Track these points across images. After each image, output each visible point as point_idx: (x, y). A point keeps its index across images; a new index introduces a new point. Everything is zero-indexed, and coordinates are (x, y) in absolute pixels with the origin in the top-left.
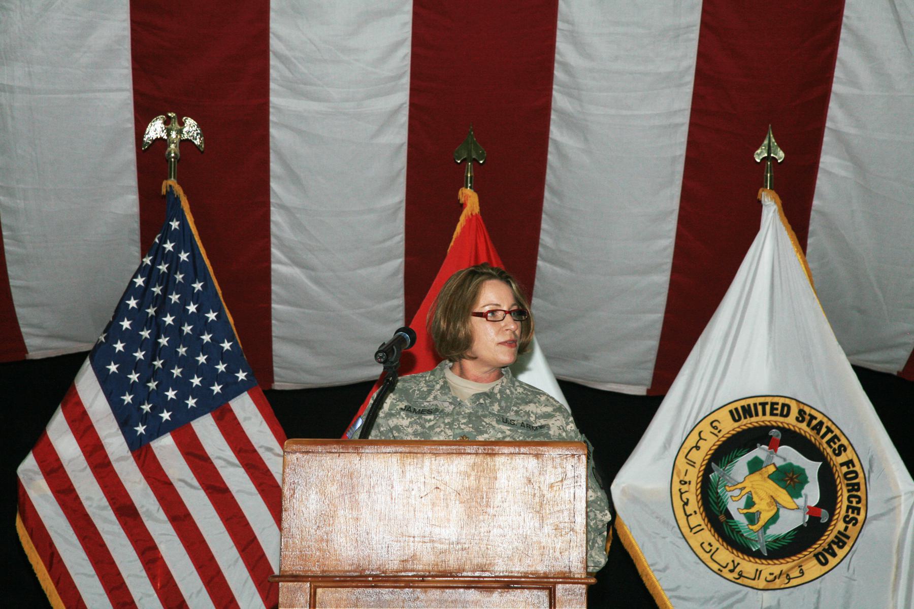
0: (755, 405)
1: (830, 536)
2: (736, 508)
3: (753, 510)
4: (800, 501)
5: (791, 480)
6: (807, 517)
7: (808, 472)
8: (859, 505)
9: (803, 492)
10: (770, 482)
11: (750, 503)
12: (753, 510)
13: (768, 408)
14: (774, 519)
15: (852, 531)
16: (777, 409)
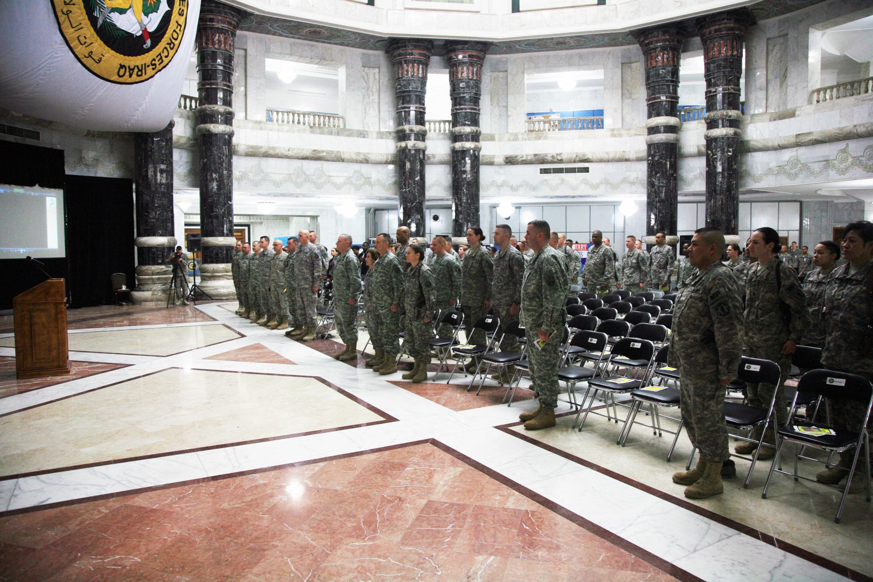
4: (145, 20)
8: (164, 59)
14: (122, 11)
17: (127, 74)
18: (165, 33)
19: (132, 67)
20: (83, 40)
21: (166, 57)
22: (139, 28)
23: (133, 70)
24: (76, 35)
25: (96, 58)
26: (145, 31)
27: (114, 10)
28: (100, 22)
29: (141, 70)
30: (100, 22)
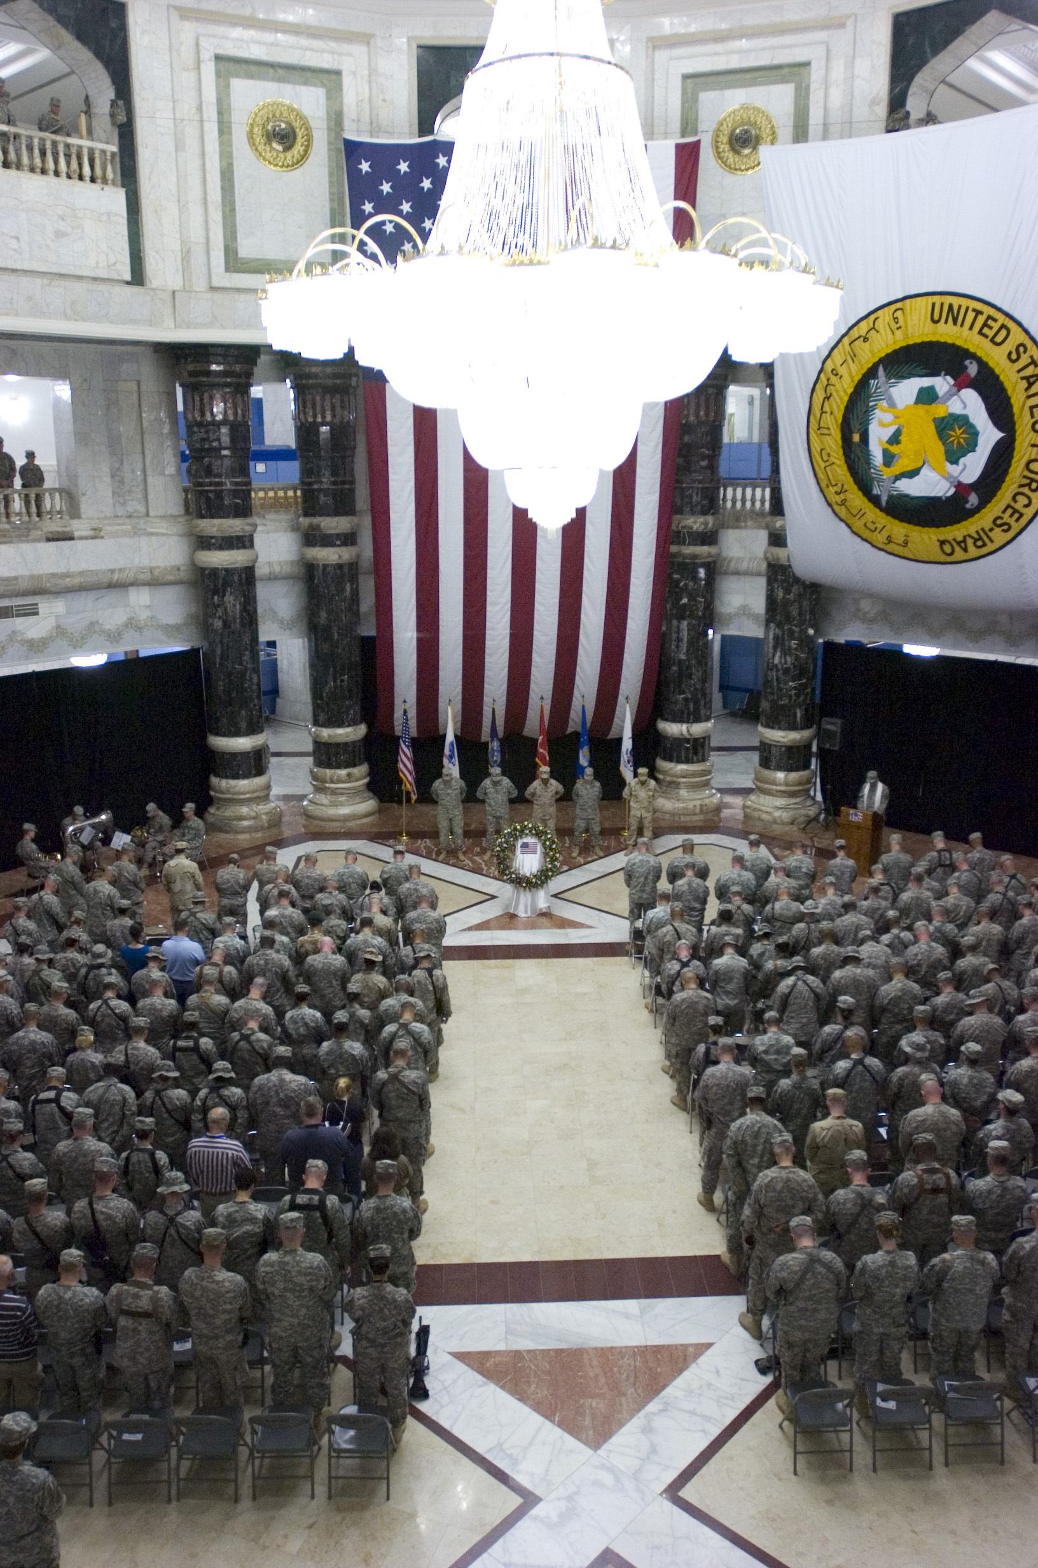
0: (967, 308)
1: (969, 527)
2: (878, 434)
3: (894, 449)
4: (954, 470)
5: (954, 436)
6: (952, 491)
7: (981, 440)
8: (1024, 510)
9: (962, 460)
10: (932, 426)
11: (895, 439)
12: (894, 449)
13: (981, 320)
15: (999, 537)
16: (991, 328)
17: (957, 549)
18: (1005, 472)
19: (960, 539)
20: (870, 525)
21: (1026, 506)
22: (948, 485)
23: (964, 541)
24: (863, 521)
25: (901, 542)
26: (959, 486)
27: (897, 478)
28: (884, 499)
29: (980, 540)
30: (884, 499)
